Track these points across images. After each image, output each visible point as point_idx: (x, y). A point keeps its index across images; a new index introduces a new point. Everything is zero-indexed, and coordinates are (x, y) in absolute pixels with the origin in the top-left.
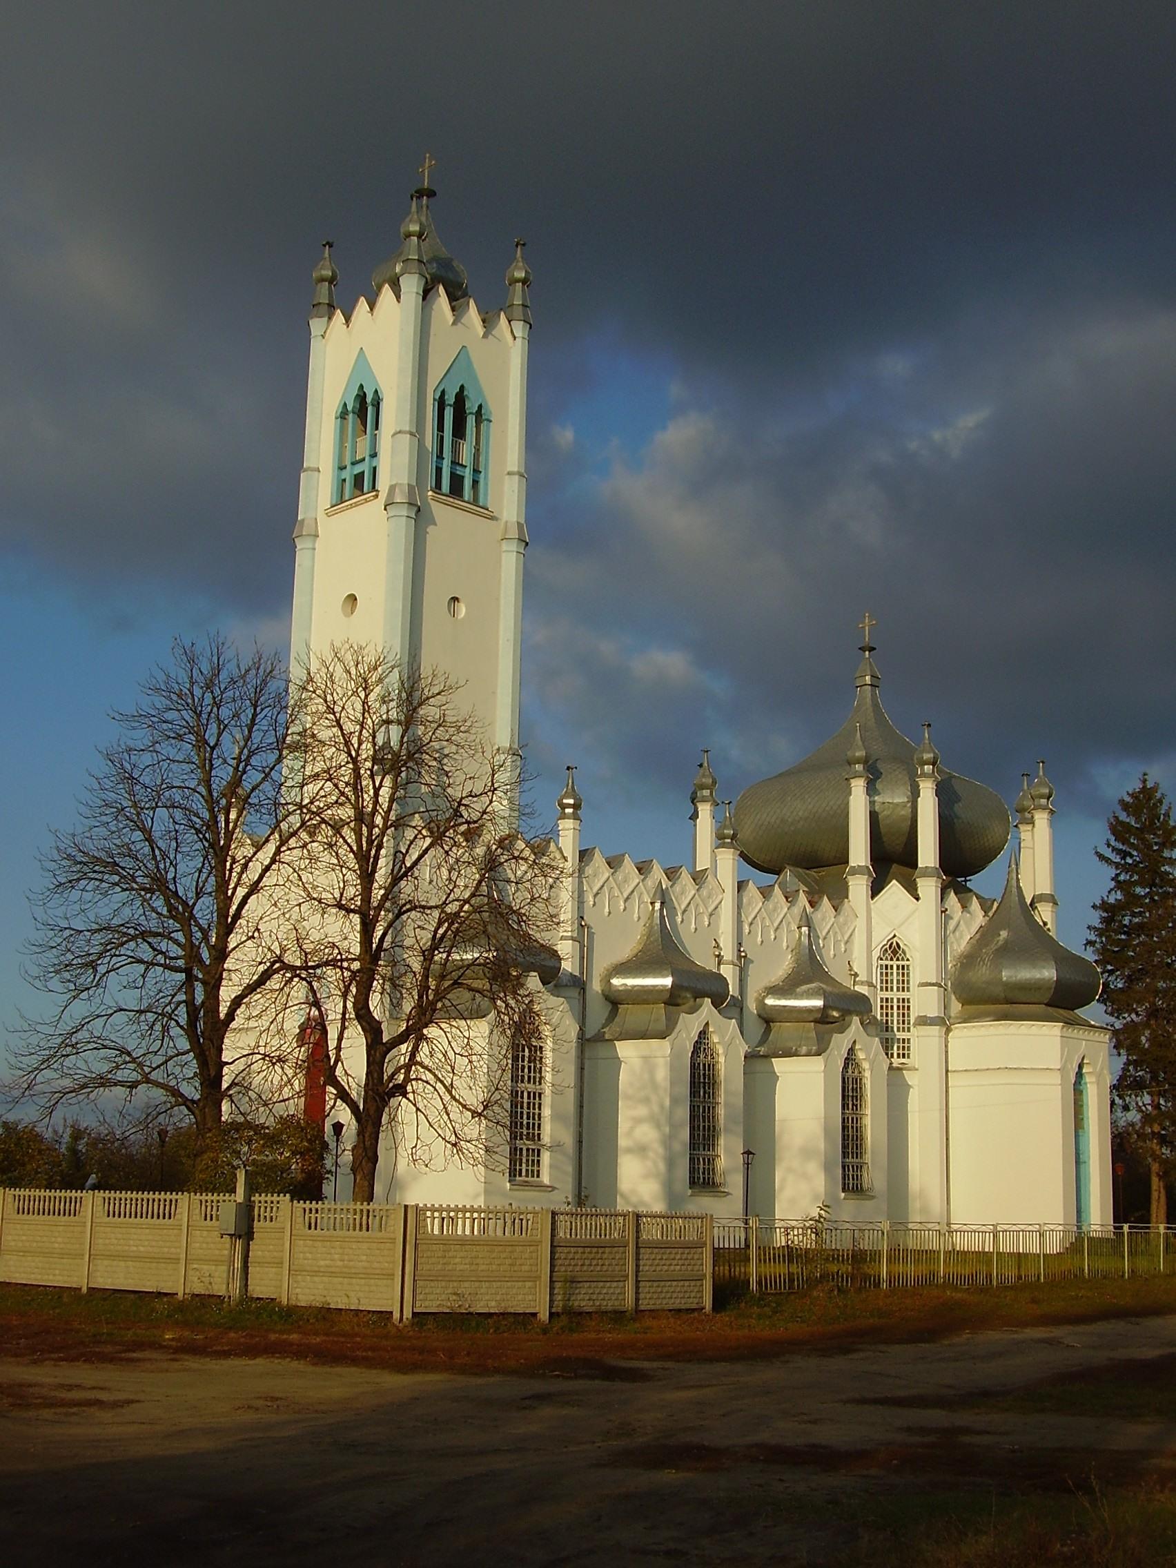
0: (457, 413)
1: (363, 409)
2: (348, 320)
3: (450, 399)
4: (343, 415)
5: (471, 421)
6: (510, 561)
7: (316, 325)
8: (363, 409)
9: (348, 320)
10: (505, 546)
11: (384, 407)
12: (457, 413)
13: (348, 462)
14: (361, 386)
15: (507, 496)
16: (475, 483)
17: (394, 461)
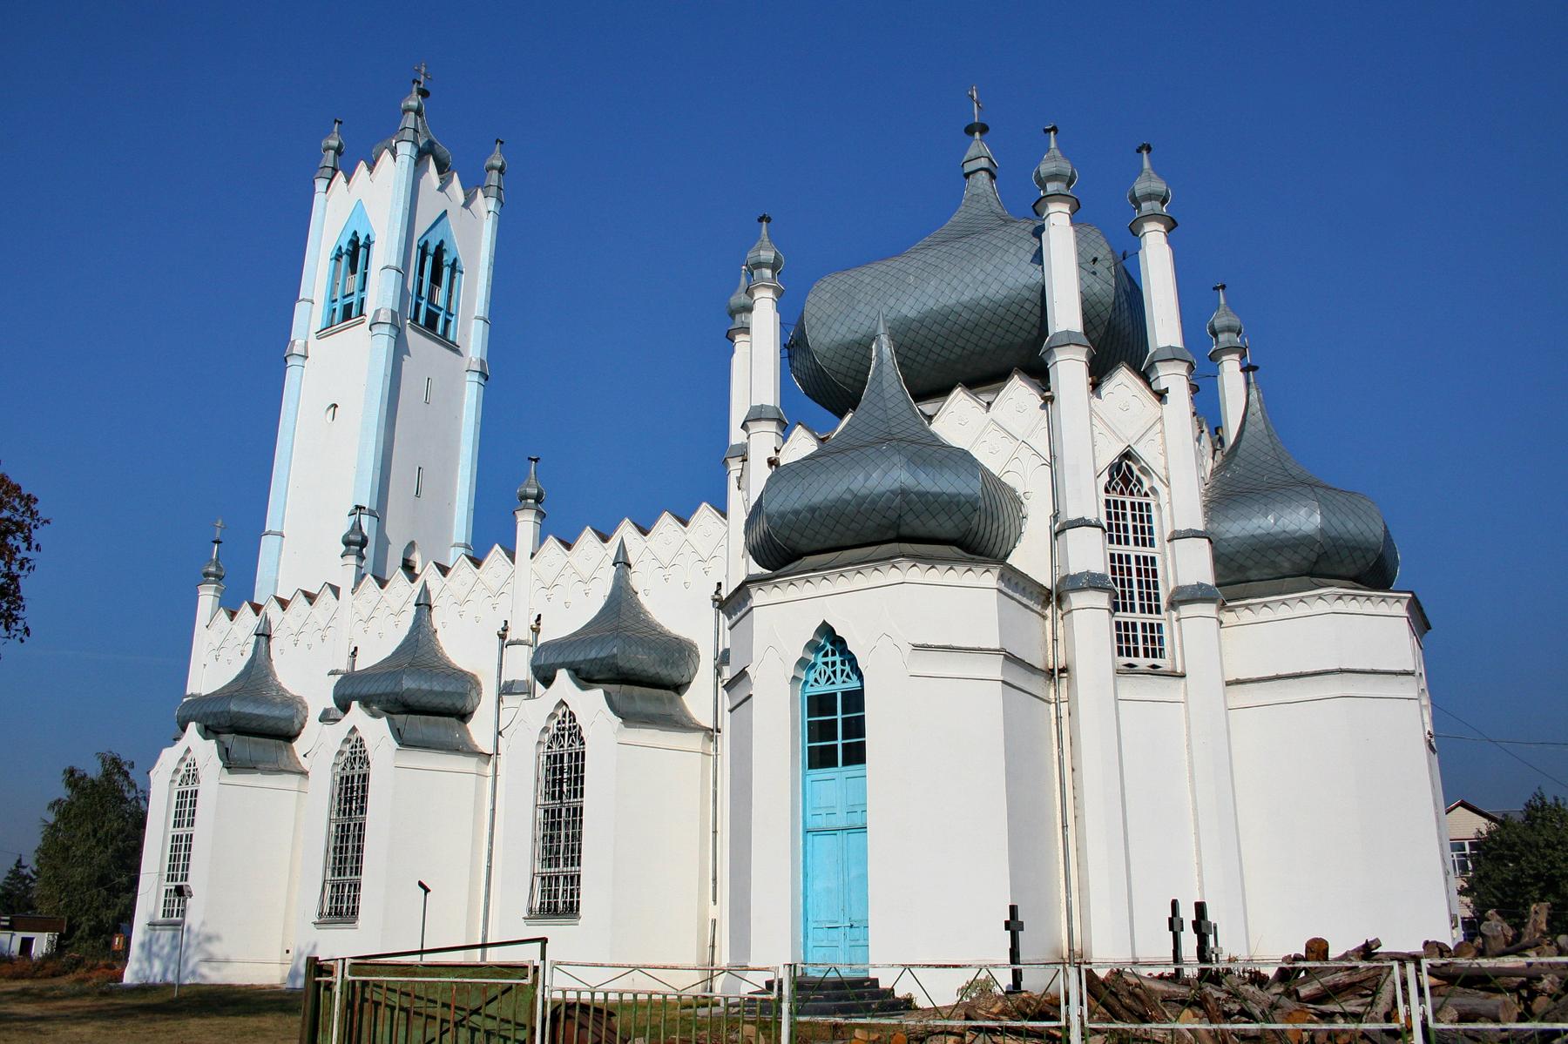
0: (433, 263)
1: (355, 253)
2: (348, 181)
3: (432, 249)
4: (338, 258)
5: (446, 272)
6: (471, 392)
7: (320, 185)
8: (355, 253)
9: (348, 181)
10: (469, 376)
11: (374, 249)
12: (433, 263)
13: (338, 296)
14: (355, 233)
15: (473, 336)
16: (447, 322)
17: (381, 292)
